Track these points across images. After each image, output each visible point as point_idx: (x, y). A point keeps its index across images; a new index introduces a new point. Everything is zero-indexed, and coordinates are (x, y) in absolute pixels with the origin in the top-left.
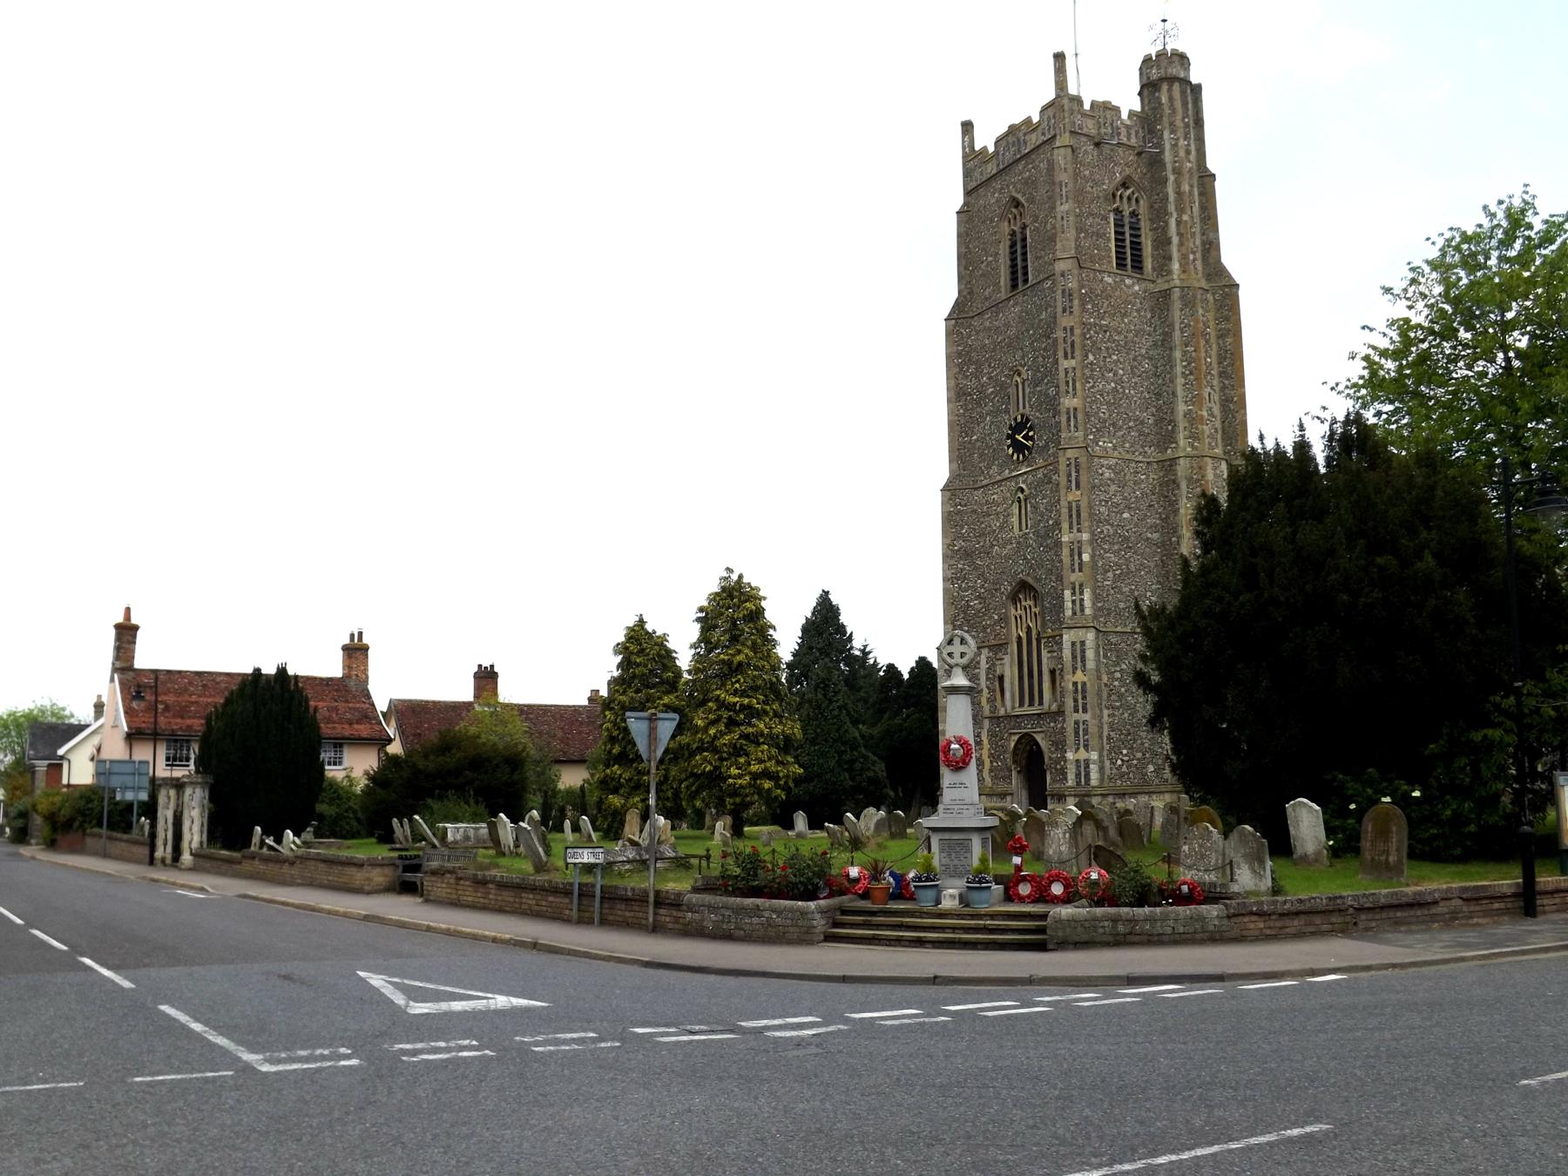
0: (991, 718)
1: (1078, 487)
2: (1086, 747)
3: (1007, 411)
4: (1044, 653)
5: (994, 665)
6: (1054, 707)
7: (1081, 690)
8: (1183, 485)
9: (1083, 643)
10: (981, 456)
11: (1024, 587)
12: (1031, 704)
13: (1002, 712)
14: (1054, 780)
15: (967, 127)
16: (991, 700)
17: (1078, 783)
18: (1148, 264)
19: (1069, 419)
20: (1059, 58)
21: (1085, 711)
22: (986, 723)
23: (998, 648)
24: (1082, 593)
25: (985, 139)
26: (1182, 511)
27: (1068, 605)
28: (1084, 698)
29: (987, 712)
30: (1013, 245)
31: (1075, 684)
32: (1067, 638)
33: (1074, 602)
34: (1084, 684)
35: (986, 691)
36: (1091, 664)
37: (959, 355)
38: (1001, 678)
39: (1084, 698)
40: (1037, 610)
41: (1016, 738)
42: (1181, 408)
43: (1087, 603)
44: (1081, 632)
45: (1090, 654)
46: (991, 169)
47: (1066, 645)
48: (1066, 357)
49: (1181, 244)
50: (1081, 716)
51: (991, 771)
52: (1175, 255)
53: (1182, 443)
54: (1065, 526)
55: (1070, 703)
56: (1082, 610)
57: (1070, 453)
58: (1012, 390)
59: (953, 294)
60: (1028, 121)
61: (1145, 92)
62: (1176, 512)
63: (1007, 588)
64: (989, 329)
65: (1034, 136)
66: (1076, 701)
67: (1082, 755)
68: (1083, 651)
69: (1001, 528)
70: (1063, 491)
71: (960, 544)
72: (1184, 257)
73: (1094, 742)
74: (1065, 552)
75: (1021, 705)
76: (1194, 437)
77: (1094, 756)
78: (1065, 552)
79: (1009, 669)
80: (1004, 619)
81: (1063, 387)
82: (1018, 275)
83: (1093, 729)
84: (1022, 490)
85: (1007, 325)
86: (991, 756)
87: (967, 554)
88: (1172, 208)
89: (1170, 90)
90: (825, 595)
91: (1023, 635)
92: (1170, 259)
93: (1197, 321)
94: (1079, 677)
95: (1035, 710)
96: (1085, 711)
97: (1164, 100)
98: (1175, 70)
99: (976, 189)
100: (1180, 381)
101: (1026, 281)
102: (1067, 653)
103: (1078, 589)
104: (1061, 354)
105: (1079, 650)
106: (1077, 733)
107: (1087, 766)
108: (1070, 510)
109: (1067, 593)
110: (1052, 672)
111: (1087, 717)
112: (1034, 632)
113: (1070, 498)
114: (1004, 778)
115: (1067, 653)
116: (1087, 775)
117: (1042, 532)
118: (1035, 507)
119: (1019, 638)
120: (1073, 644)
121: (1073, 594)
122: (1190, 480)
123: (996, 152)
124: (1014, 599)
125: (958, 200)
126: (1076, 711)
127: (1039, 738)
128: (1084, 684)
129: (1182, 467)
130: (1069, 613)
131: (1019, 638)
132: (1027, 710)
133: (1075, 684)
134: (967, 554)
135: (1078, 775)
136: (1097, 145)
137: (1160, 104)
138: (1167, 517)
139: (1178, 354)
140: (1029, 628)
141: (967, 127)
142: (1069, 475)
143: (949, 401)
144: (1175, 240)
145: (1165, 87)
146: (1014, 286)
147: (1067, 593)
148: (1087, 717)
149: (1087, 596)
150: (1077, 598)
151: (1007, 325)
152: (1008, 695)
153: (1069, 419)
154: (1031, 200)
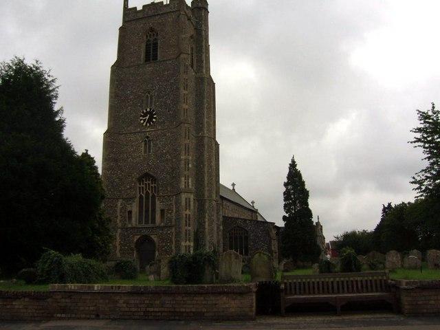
0: (122, 229)
4: (158, 202)
7: (188, 217)
8: (206, 146)
9: (189, 199)
11: (147, 176)
12: (147, 222)
13: (130, 226)
22: (119, 231)
23: (129, 199)
28: (189, 220)
30: (148, 46)
31: (186, 215)
32: (184, 196)
33: (185, 183)
34: (189, 215)
35: (119, 217)
36: (192, 207)
38: (130, 212)
39: (189, 220)
41: (138, 237)
42: (206, 120)
44: (189, 195)
45: (192, 203)
46: (140, 16)
47: (183, 200)
58: (144, 98)
59: (115, 59)
63: (136, 175)
68: (190, 201)
71: (112, 155)
75: (140, 222)
77: (192, 244)
78: (183, 162)
79: (135, 208)
82: (151, 54)
84: (147, 137)
86: (120, 244)
88: (204, 51)
92: (202, 67)
94: (188, 212)
95: (150, 225)
99: (128, 21)
100: (205, 110)
102: (183, 203)
103: (187, 178)
105: (188, 200)
109: (183, 178)
110: (162, 211)
111: (189, 228)
112: (151, 195)
113: (186, 142)
115: (183, 203)
118: (155, 145)
119: (141, 197)
120: (186, 199)
122: (208, 145)
124: (140, 180)
127: (153, 237)
128: (189, 215)
132: (143, 225)
133: (186, 215)
134: (116, 160)
137: (201, 16)
138: (199, 158)
140: (147, 194)
146: (147, 59)
148: (189, 228)
149: (190, 181)
152: (133, 219)
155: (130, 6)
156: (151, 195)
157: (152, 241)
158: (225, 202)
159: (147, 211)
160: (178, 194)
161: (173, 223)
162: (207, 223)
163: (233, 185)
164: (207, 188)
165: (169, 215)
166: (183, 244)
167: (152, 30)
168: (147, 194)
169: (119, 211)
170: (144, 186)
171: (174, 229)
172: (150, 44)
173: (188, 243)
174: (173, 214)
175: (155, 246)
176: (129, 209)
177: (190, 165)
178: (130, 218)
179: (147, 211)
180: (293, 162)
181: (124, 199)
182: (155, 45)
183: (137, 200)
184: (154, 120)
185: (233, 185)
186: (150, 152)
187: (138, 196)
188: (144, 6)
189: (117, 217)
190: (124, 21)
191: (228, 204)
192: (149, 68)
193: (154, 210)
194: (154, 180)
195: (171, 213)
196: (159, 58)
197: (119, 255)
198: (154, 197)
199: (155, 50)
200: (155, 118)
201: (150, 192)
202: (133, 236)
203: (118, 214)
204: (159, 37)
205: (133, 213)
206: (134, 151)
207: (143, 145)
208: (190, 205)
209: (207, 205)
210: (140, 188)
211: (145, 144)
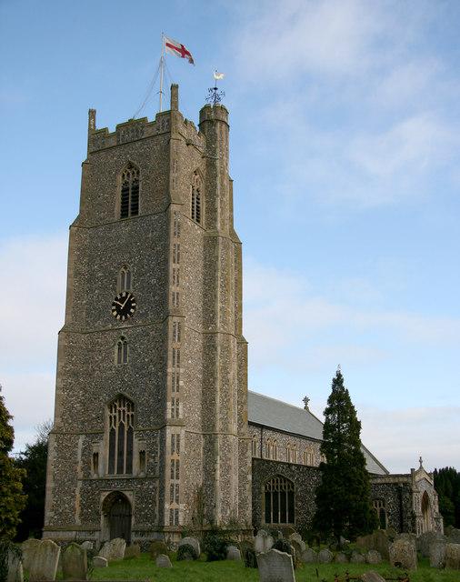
1: (179, 340)
2: (177, 501)
3: (114, 289)
4: (135, 440)
5: (89, 446)
6: (142, 475)
8: (219, 348)
9: (178, 435)
10: (87, 314)
11: (121, 398)
12: (120, 470)
13: (95, 476)
14: (138, 522)
15: (92, 113)
16: (86, 469)
17: (171, 524)
18: (203, 219)
19: (174, 299)
20: (174, 88)
21: (178, 478)
22: (80, 484)
23: (95, 435)
24: (178, 405)
25: (109, 121)
26: (218, 364)
27: (169, 411)
28: (178, 469)
29: (81, 475)
30: (125, 191)
31: (172, 461)
32: (169, 431)
33: (173, 409)
35: (81, 463)
37: (79, 249)
38: (96, 455)
39: (178, 469)
40: (130, 413)
41: (107, 494)
42: (219, 305)
43: (180, 411)
45: (182, 442)
46: (113, 142)
48: (174, 262)
49: (222, 214)
50: (175, 481)
51: (81, 515)
52: (219, 219)
53: (219, 325)
54: (170, 363)
55: (168, 472)
56: (177, 416)
57: (176, 319)
60: (144, 119)
61: (206, 125)
62: (214, 364)
63: (105, 397)
64: (103, 237)
65: (150, 130)
66: (172, 471)
67: (175, 505)
68: (178, 441)
69: (102, 361)
70: (170, 342)
72: (223, 221)
73: (181, 498)
74: (169, 378)
75: (111, 471)
76: (224, 322)
77: (182, 506)
79: (103, 448)
80: (101, 418)
81: (171, 279)
82: (130, 204)
83: (182, 490)
84: (123, 338)
85: (118, 237)
87: (75, 374)
88: (218, 192)
89: (221, 127)
90: (338, 381)
91: (117, 429)
92: (216, 220)
93: (229, 258)
94: (175, 457)
95: (125, 475)
96: (178, 478)
97: (218, 131)
98: (222, 117)
100: (219, 290)
101: (135, 212)
104: (171, 259)
106: (172, 492)
107: (177, 513)
108: (174, 354)
110: (142, 453)
111: (179, 482)
112: (126, 429)
114: (93, 520)
116: (177, 518)
117: (139, 365)
118: (133, 350)
119: (113, 430)
120: (173, 436)
121: (173, 405)
122: (222, 346)
123: (117, 134)
125: (84, 156)
126: (172, 478)
127: (127, 494)
129: (219, 338)
130: (169, 416)
131: (113, 430)
133: (172, 461)
134: (75, 374)
135: (171, 519)
136: (188, 145)
138: (208, 366)
139: (219, 274)
140: (122, 424)
141: (92, 113)
142: (175, 332)
143: (69, 276)
144: (219, 210)
145: (219, 125)
146: (124, 214)
147: (169, 404)
148: (179, 482)
149: (181, 407)
150: (175, 407)
151: (118, 237)
152: (100, 466)
153: (174, 299)
154: (146, 167)
155: (99, 127)
156: (126, 429)
157: (125, 500)
158: (268, 433)
159: (121, 454)
160: (163, 428)
161: (157, 473)
162: (218, 472)
163: (306, 400)
164: (219, 416)
165: (151, 460)
166: (167, 506)
167: (131, 166)
168: (122, 424)
169: (80, 452)
170: (117, 414)
171: (158, 482)
172: (128, 189)
173: (175, 505)
174: (157, 459)
175: (130, 506)
176: (95, 451)
177: (181, 383)
178: (96, 464)
179: (121, 454)
180: (339, 376)
181: (86, 434)
182: (136, 189)
183: (107, 436)
184: (132, 310)
185: (306, 400)
186: (125, 361)
187: (108, 430)
188: (119, 127)
189: (76, 463)
190: (90, 153)
191: (278, 436)
192: (125, 229)
193: (130, 453)
194: (132, 405)
195: (154, 458)
196: (140, 211)
197: (78, 521)
198: (130, 432)
199: (135, 198)
200: (134, 308)
201: (125, 423)
202: (99, 494)
203: (79, 457)
204: (141, 178)
205: (100, 457)
206: (102, 361)
207: (117, 351)
208: (178, 446)
209: (219, 442)
210: (111, 417)
211: (120, 349)
